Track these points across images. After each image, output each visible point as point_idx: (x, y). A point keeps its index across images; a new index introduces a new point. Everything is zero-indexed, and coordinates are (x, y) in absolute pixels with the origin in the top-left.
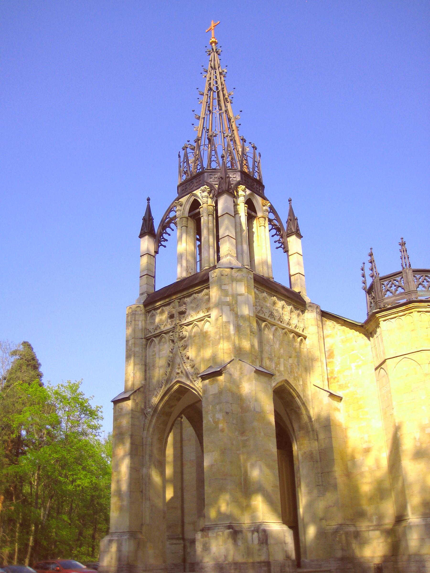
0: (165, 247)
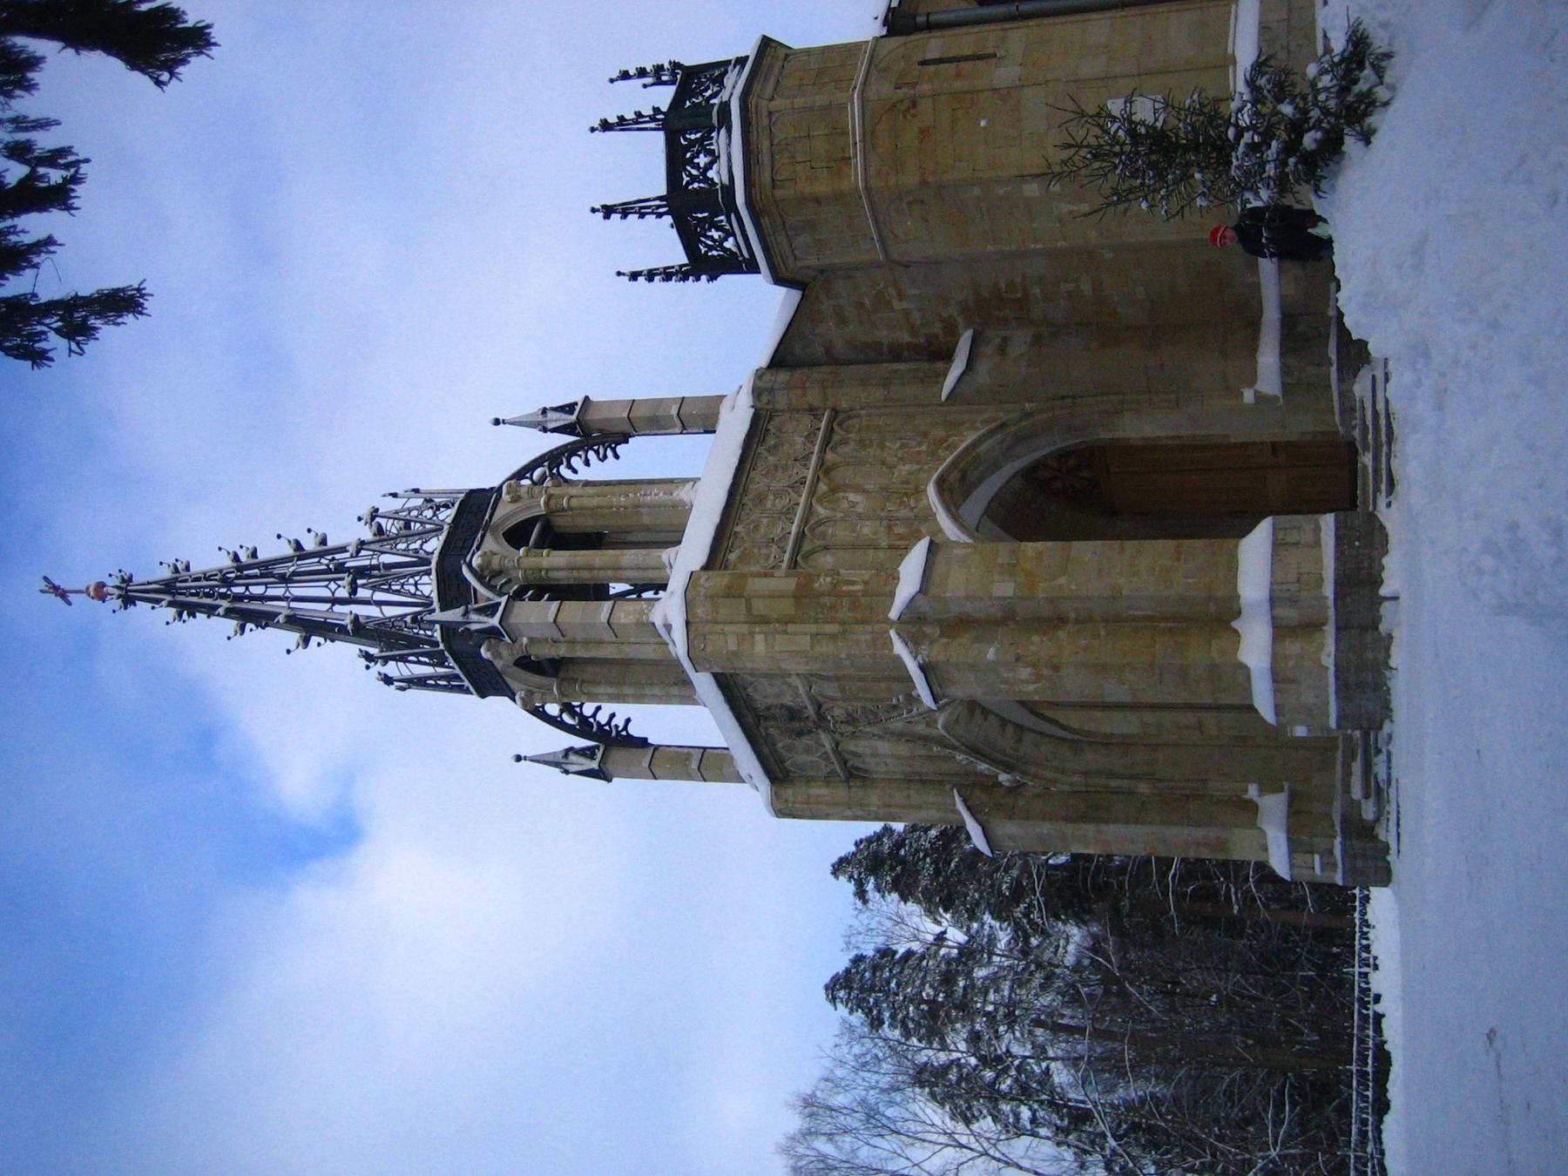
0: (628, 721)
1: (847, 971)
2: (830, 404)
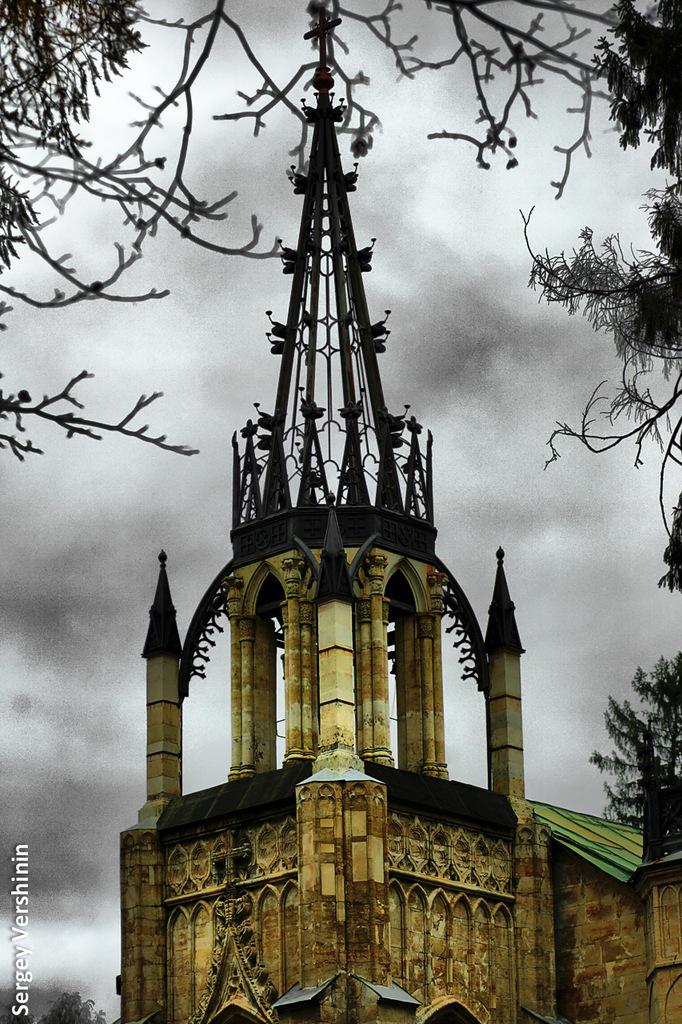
2: (519, 898)
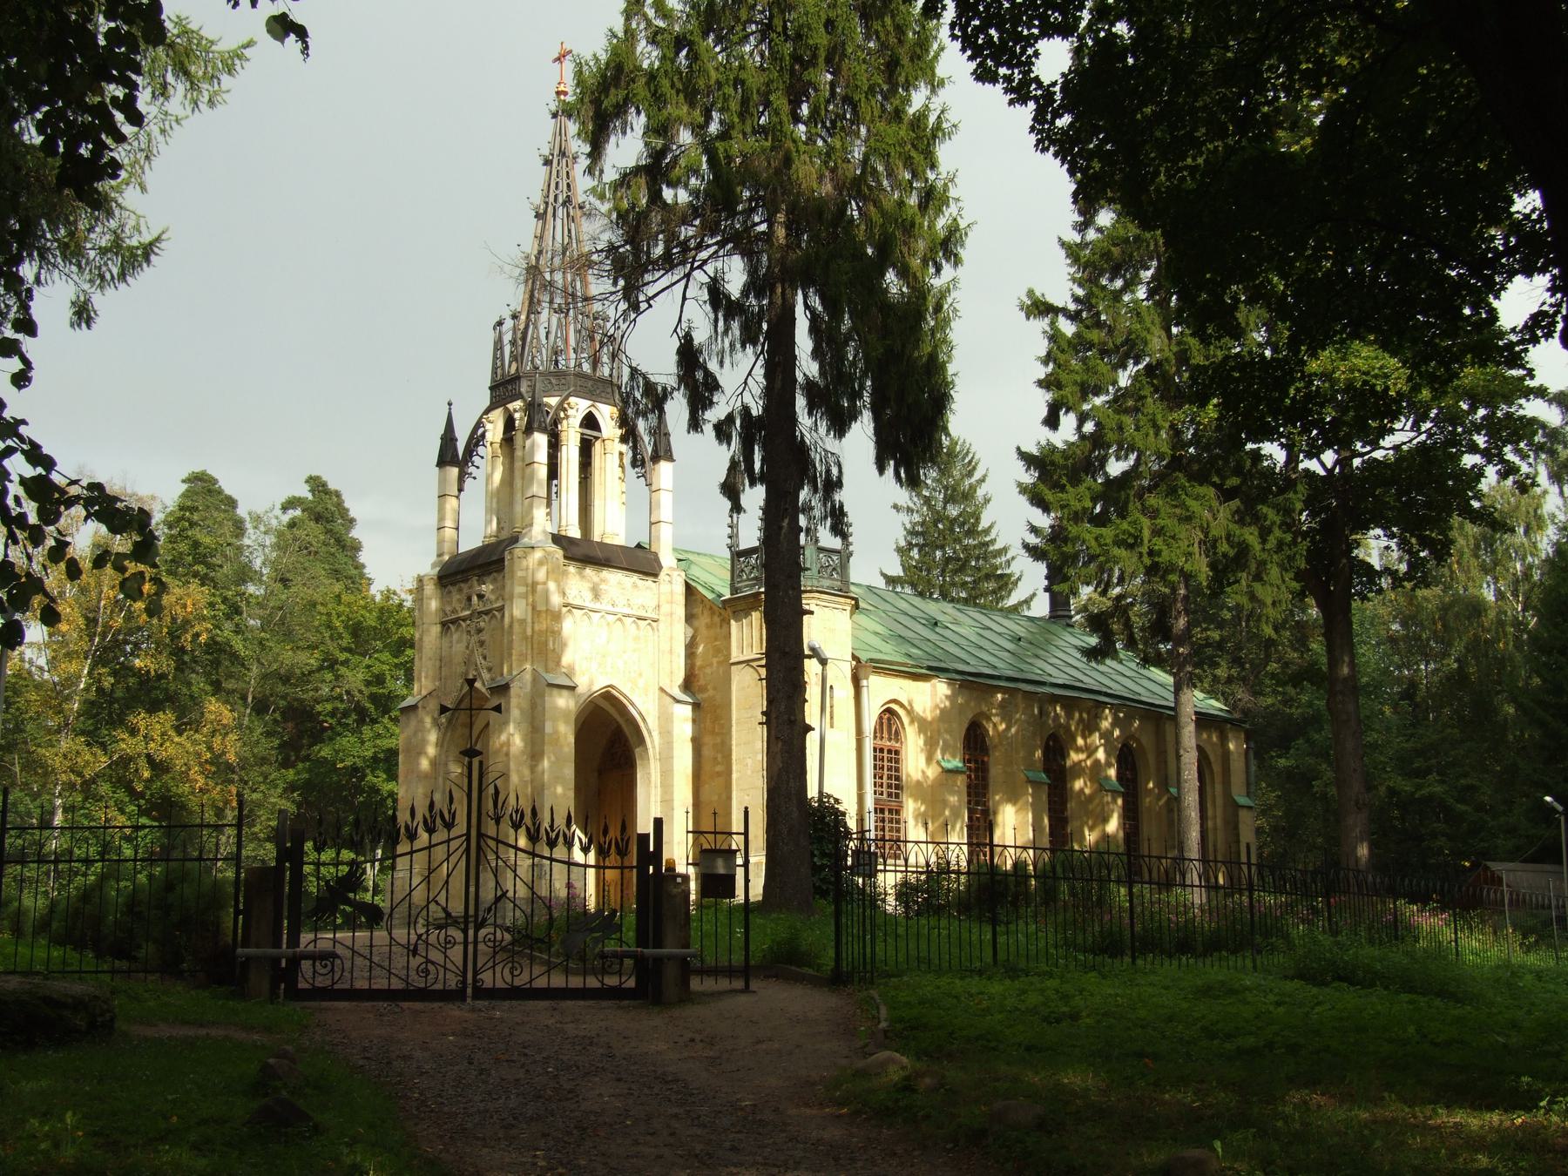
1: (220, 492)
